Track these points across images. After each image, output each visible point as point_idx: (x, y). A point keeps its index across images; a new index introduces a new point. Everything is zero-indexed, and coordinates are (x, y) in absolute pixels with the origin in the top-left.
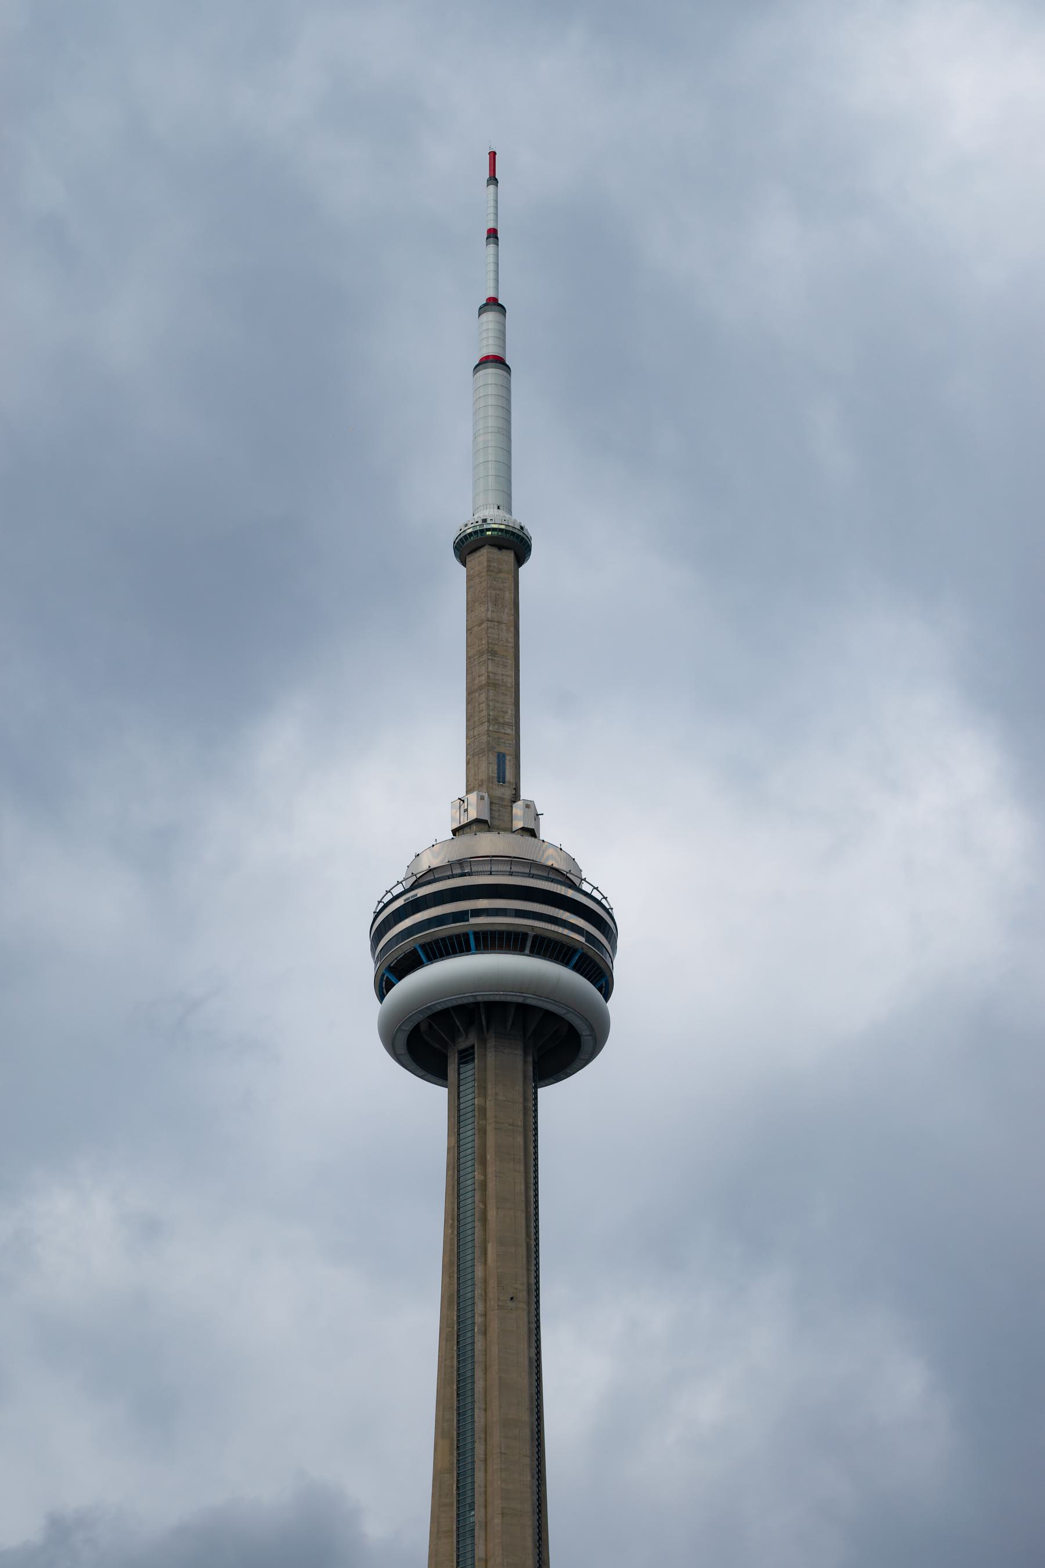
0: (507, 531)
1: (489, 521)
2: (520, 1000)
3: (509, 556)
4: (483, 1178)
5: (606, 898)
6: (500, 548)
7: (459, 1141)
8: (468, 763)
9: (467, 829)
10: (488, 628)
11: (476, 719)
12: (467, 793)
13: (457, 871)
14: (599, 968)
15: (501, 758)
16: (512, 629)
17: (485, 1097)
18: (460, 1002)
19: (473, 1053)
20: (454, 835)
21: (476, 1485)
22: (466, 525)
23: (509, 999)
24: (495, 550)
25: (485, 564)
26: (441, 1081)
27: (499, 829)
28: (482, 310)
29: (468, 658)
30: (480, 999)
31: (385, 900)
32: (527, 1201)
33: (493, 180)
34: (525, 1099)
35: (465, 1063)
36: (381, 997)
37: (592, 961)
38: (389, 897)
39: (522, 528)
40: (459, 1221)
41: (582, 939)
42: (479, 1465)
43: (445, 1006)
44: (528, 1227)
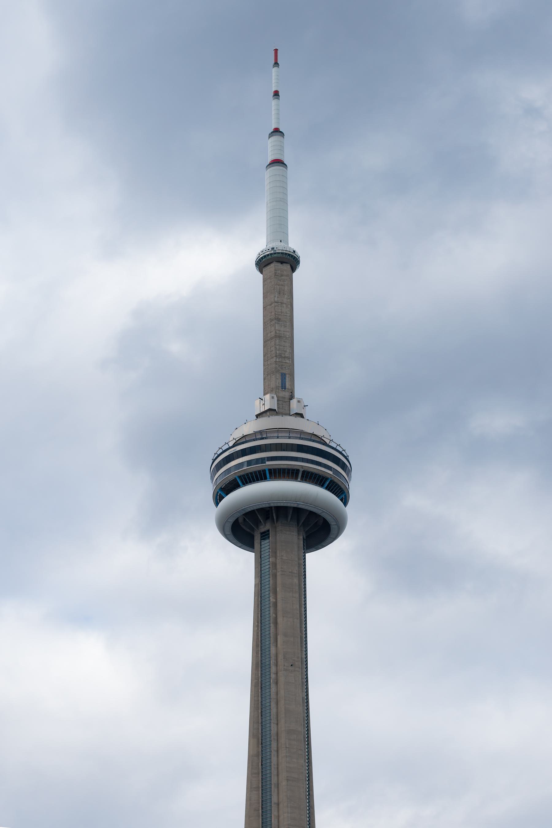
0: (286, 254)
1: (275, 249)
2: (295, 506)
3: (287, 267)
4: (274, 600)
5: (344, 451)
6: (282, 263)
7: (261, 581)
8: (264, 379)
9: (264, 414)
10: (275, 306)
11: (269, 355)
12: (264, 395)
13: (259, 436)
14: (341, 488)
15: (283, 376)
16: (289, 306)
17: (276, 558)
18: (261, 507)
19: (269, 534)
20: (257, 417)
21: (272, 764)
22: (262, 251)
23: (289, 505)
24: (279, 264)
26: (251, 549)
27: (283, 414)
28: (271, 135)
29: (264, 323)
30: (272, 505)
31: (219, 453)
32: (301, 614)
33: (276, 64)
34: (299, 559)
35: (263, 539)
36: (217, 504)
37: (337, 484)
38: (221, 451)
39: (294, 251)
40: (261, 623)
41: (331, 473)
42: (274, 753)
43: (252, 509)
44: (301, 627)
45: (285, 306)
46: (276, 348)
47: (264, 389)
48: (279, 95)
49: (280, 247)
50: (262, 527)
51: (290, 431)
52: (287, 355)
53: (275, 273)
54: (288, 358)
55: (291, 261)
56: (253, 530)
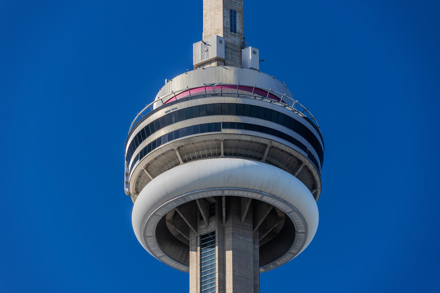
50: (203, 227)
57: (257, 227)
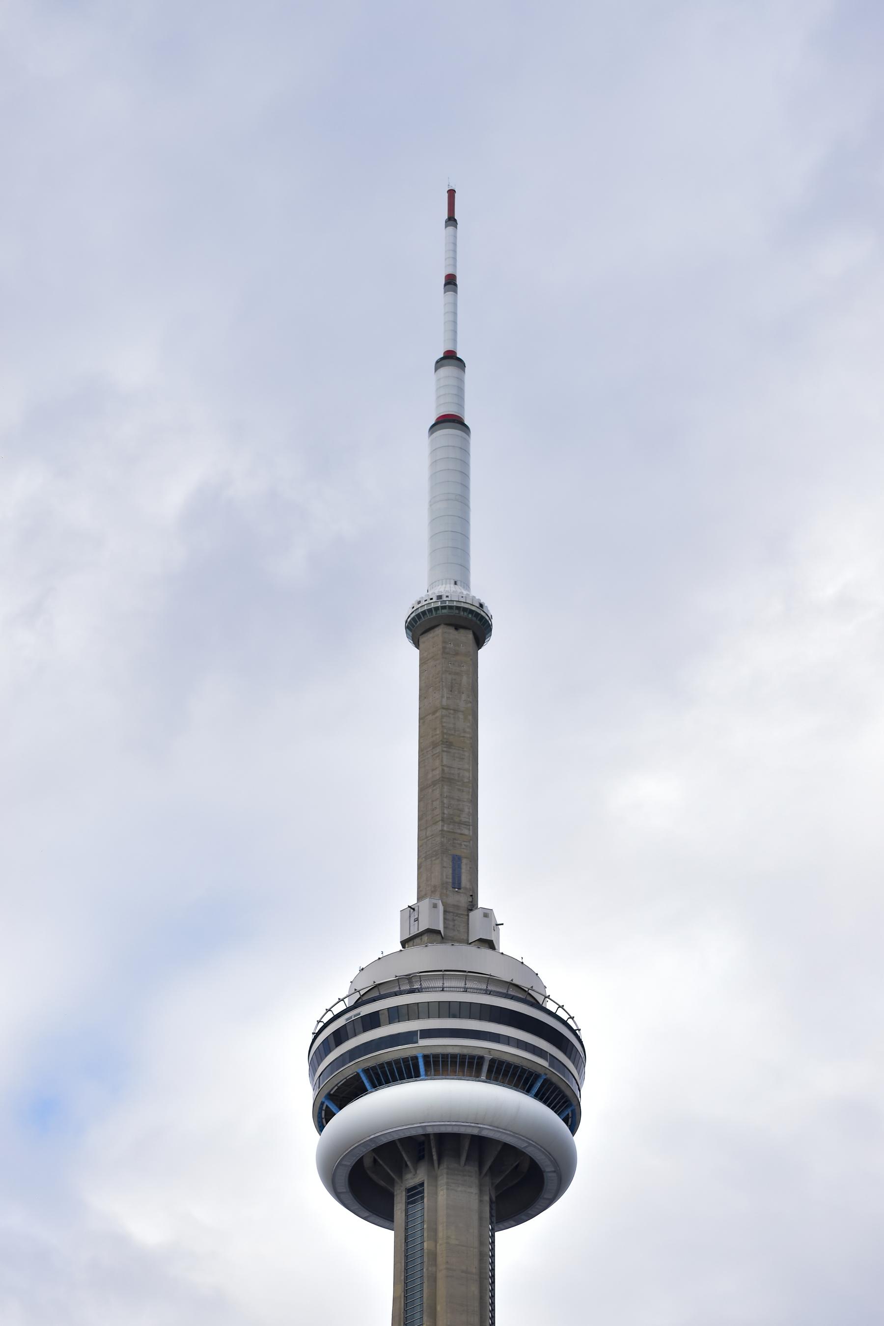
0: (465, 609)
1: (444, 598)
2: (475, 1132)
5: (572, 1018)
7: (406, 1291)
8: (419, 867)
9: (417, 940)
10: (443, 717)
12: (419, 899)
14: (564, 1096)
15: (456, 861)
16: (470, 717)
17: (436, 1242)
18: (408, 1134)
19: (422, 1192)
20: (404, 947)
22: (419, 602)
23: (462, 1130)
24: (452, 630)
25: (440, 646)
26: (387, 1223)
28: (439, 364)
30: (430, 1130)
31: (325, 1020)
33: (451, 220)
36: (320, 1127)
37: (557, 1088)
38: (329, 1016)
39: (481, 605)
41: (545, 1064)
43: (390, 1139)
45: (461, 716)
46: (442, 802)
47: (419, 887)
48: (455, 285)
49: (450, 592)
50: (409, 1176)
51: (467, 975)
52: (464, 818)
53: (444, 648)
54: (466, 824)
55: (474, 625)
56: (392, 1182)
57: (486, 1168)
